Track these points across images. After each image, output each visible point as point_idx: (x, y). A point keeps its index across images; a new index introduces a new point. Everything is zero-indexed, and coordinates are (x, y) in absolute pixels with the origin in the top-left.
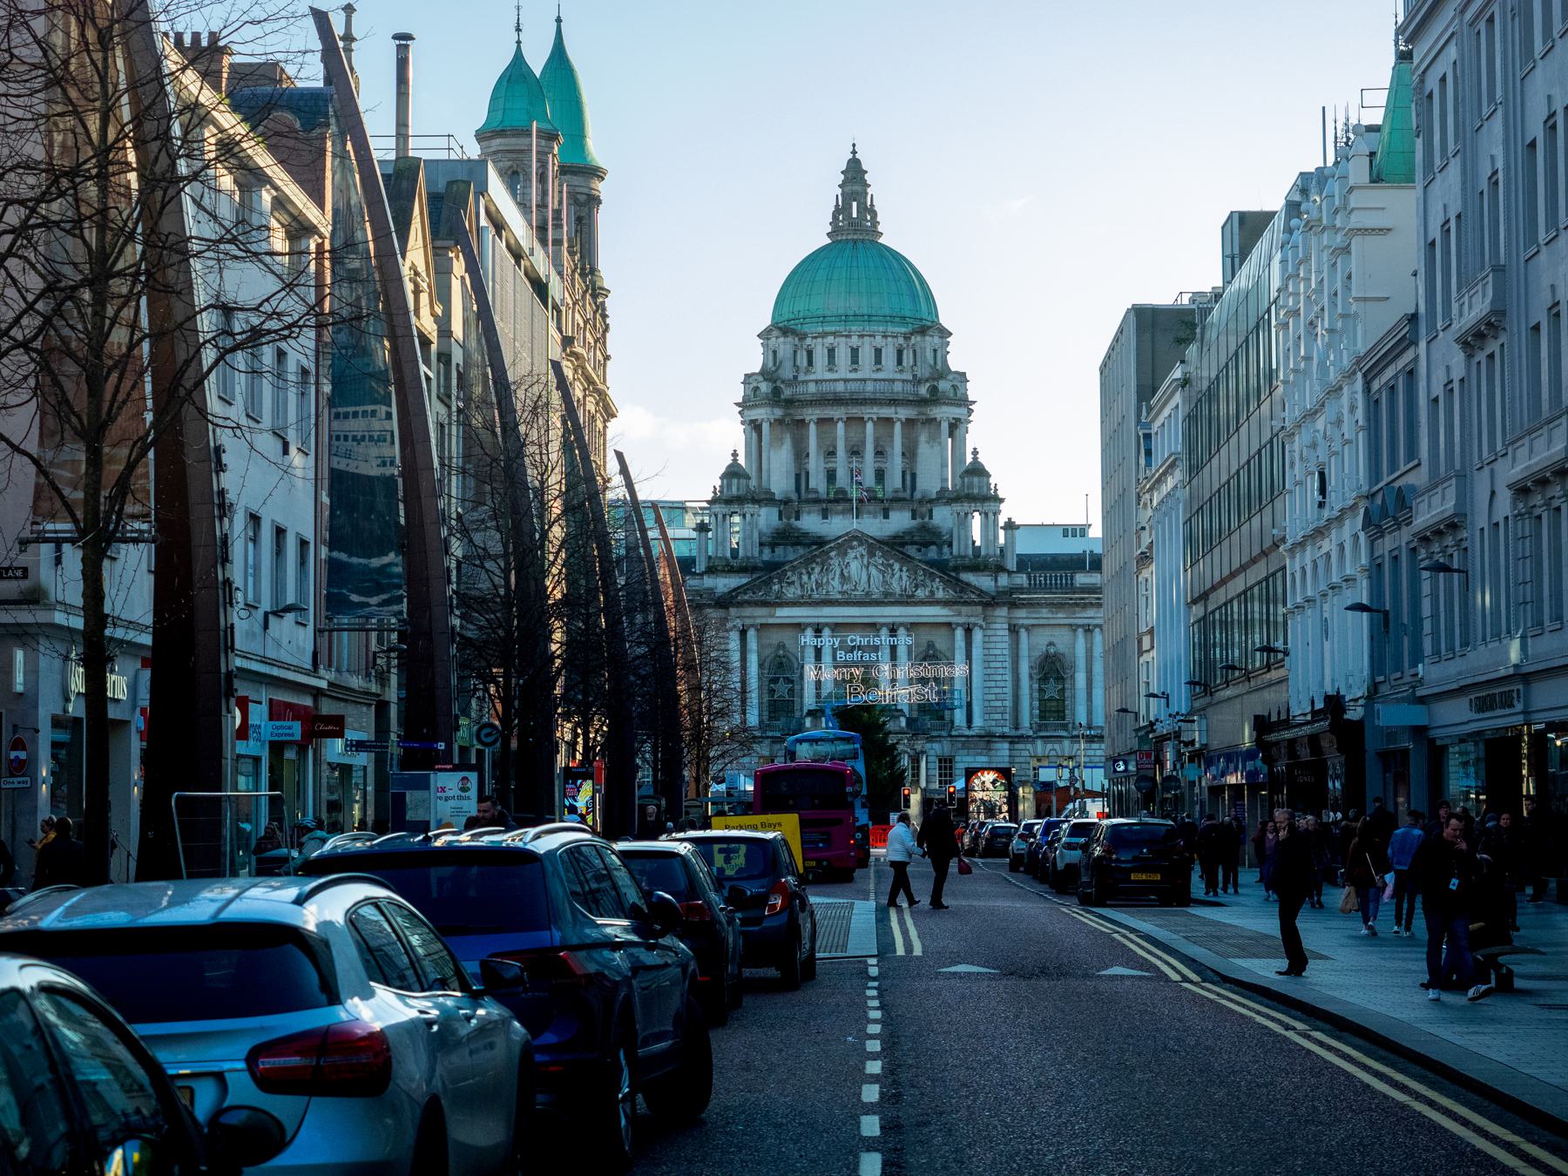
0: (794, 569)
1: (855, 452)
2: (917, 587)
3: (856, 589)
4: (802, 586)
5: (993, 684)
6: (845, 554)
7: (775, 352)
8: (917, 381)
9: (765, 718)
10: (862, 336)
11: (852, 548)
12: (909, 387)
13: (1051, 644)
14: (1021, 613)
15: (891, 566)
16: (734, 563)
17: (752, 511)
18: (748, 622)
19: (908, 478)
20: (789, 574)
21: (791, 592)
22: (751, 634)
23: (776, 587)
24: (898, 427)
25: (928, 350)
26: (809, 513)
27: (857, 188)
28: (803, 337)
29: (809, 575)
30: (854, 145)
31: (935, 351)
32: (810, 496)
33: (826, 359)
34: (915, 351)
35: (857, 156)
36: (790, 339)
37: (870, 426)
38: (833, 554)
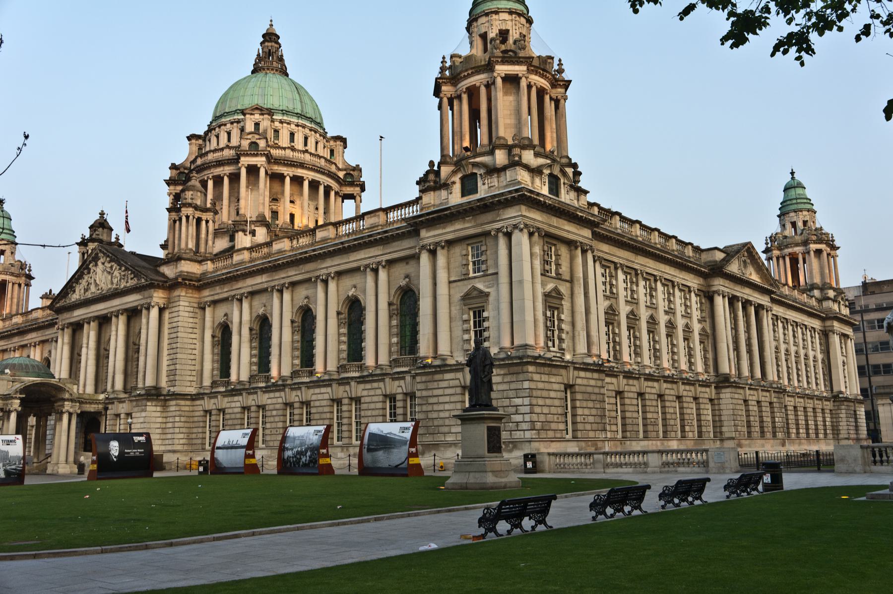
10: (219, 127)
24: (226, 180)
30: (271, 21)
38: (91, 266)
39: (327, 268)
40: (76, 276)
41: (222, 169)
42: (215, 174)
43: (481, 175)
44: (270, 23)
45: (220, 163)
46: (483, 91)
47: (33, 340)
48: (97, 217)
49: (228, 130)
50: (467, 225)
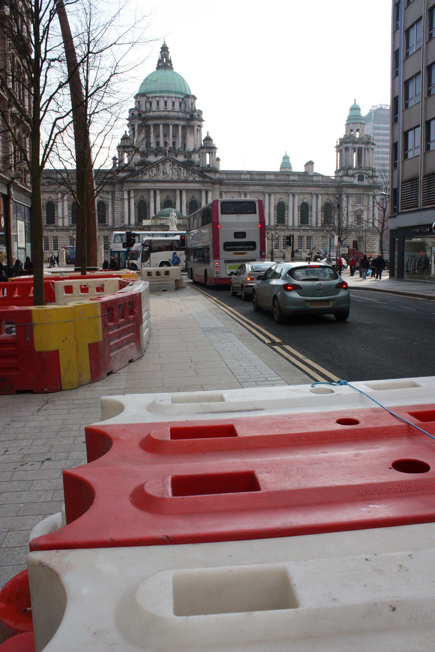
0: (146, 170)
3: (168, 177)
4: (149, 176)
6: (164, 165)
7: (139, 103)
8: (187, 113)
9: (137, 221)
11: (167, 162)
12: (184, 115)
14: (223, 187)
15: (180, 169)
18: (130, 188)
19: (183, 145)
21: (146, 177)
23: (140, 176)
24: (180, 127)
26: (151, 155)
29: (152, 171)
31: (192, 104)
32: (151, 150)
34: (185, 104)
35: (165, 43)
36: (144, 98)
37: (171, 127)
38: (160, 164)
39: (295, 190)
43: (366, 177)
44: (164, 41)
45: (179, 119)
46: (363, 150)
48: (124, 133)
49: (174, 101)
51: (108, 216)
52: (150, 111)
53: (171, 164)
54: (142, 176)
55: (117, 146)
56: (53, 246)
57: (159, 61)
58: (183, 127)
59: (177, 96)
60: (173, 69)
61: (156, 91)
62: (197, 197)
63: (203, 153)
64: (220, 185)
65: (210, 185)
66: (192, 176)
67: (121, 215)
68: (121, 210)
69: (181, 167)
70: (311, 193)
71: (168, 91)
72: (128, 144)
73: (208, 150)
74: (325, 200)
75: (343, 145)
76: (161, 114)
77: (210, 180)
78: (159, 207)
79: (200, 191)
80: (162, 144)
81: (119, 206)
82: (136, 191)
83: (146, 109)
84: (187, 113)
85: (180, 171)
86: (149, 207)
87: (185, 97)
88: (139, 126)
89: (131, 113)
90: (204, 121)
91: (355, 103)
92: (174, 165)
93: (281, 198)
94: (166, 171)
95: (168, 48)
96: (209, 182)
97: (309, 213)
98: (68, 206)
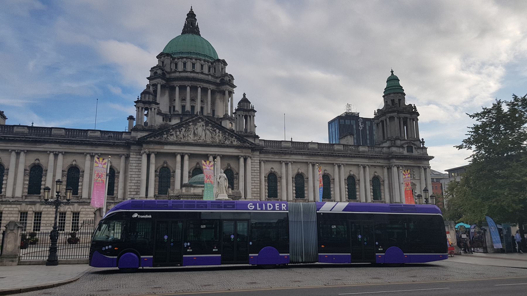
0: (173, 129)
1: (193, 100)
2: (225, 140)
3: (200, 139)
4: (177, 137)
5: (253, 182)
6: (196, 125)
7: (163, 62)
8: (217, 78)
9: (157, 194)
11: (199, 122)
13: (272, 168)
14: (262, 156)
15: (215, 131)
16: (146, 128)
17: (155, 107)
18: (151, 150)
20: (171, 130)
22: (153, 156)
24: (209, 92)
25: (220, 67)
26: (175, 119)
27: (194, 19)
28: (174, 59)
29: (180, 131)
30: (191, 7)
31: (222, 69)
32: (176, 113)
33: (183, 67)
34: (215, 68)
36: (169, 58)
37: (199, 89)
38: (191, 124)
39: (341, 161)
40: (174, 127)
41: (208, 85)
42: (204, 86)
44: (191, 8)
45: (208, 82)
46: (408, 120)
47: (55, 150)
48: (145, 88)
50: (411, 162)
51: (117, 186)
52: (175, 72)
53: (204, 125)
54: (168, 136)
55: (137, 100)
56: (33, 225)
57: (185, 26)
58: (213, 92)
59: (206, 59)
60: (200, 35)
61: (182, 52)
62: (233, 165)
63: (239, 115)
64: (260, 153)
65: (250, 151)
66: (229, 140)
67: (136, 184)
68: (136, 179)
69: (215, 129)
70: (358, 165)
71: (197, 53)
72: (151, 100)
73: (245, 113)
74: (373, 173)
75: (387, 115)
76: (189, 75)
77: (250, 144)
78: (187, 176)
79: (237, 158)
80: (188, 108)
81: (134, 173)
82: (158, 155)
83: (171, 70)
84: (217, 78)
85: (214, 133)
86: (174, 176)
87: (214, 62)
88: (163, 87)
89: (154, 72)
90: (235, 87)
91: (392, 74)
92: (207, 125)
93: (325, 170)
94: (197, 132)
95: (195, 15)
96: (249, 148)
97: (357, 187)
98: (63, 171)
